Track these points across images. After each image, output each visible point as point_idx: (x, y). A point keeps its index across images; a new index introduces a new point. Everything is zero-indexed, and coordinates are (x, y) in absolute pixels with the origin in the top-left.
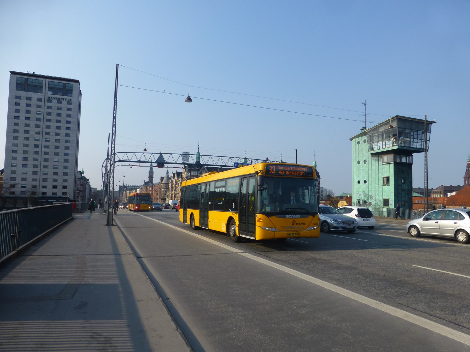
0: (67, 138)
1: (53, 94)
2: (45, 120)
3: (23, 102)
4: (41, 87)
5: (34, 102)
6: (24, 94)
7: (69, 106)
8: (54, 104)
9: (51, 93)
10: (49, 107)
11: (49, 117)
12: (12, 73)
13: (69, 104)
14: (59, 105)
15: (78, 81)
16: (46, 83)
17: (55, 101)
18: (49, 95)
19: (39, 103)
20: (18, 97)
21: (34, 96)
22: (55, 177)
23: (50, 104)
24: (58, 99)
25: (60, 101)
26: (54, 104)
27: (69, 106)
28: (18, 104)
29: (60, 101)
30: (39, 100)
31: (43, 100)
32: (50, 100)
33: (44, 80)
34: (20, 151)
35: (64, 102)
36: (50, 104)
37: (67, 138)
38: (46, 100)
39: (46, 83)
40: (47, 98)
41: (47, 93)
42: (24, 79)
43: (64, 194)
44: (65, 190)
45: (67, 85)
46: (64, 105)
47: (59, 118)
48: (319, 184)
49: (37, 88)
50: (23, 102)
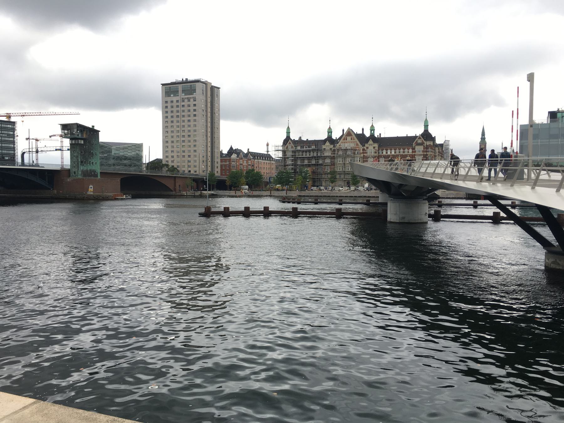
3: (169, 105)
5: (175, 104)
6: (169, 99)
7: (195, 103)
8: (186, 103)
9: (183, 94)
10: (183, 106)
12: (163, 85)
14: (189, 103)
17: (186, 100)
18: (183, 97)
20: (166, 102)
23: (183, 104)
24: (188, 98)
25: (189, 101)
26: (186, 103)
27: (195, 103)
28: (167, 107)
29: (189, 101)
30: (177, 101)
32: (183, 101)
35: (192, 100)
36: (183, 104)
49: (176, 93)
50: (169, 105)
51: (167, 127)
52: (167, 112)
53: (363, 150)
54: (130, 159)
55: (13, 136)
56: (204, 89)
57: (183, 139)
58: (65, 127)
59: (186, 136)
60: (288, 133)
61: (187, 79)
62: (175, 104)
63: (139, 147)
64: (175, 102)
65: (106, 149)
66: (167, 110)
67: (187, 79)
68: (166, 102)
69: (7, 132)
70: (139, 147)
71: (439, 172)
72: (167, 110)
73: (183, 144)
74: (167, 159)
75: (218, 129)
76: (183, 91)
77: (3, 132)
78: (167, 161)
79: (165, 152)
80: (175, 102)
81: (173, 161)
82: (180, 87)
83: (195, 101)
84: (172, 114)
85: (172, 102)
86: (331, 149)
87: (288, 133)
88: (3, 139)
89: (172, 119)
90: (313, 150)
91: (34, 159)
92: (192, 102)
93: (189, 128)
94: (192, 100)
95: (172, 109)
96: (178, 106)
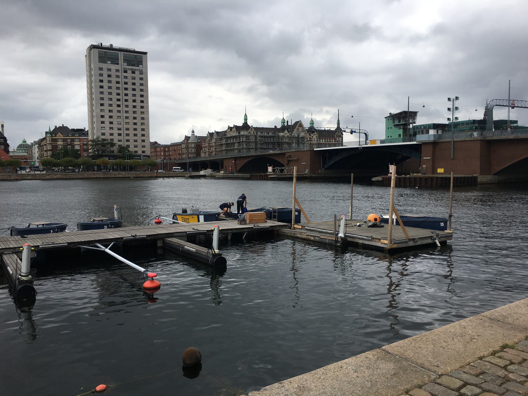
0: (142, 104)
1: (128, 65)
2: (123, 89)
4: (118, 59)
5: (113, 73)
6: (104, 66)
7: (141, 76)
8: (129, 74)
9: (126, 64)
10: (126, 77)
11: (126, 86)
13: (140, 74)
14: (133, 75)
15: (146, 53)
16: (121, 55)
17: (129, 72)
18: (125, 67)
19: (118, 74)
20: (101, 69)
21: (114, 67)
22: (136, 138)
25: (133, 72)
26: (129, 74)
27: (141, 76)
28: (101, 75)
29: (133, 72)
30: (117, 71)
31: (120, 71)
32: (125, 72)
33: (119, 52)
34: (107, 117)
36: (126, 74)
37: (142, 104)
38: (123, 71)
40: (123, 69)
41: (122, 65)
42: (103, 53)
43: (143, 152)
44: (144, 149)
45: (138, 57)
46: (137, 75)
47: (134, 87)
48: (342, 139)
49: (115, 61)
50: (105, 73)
53: (310, 138)
57: (127, 115)
60: (246, 119)
64: (113, 70)
67: (111, 45)
73: (127, 121)
76: (124, 60)
80: (113, 70)
85: (109, 70)
86: (288, 136)
87: (246, 119)
90: (271, 137)
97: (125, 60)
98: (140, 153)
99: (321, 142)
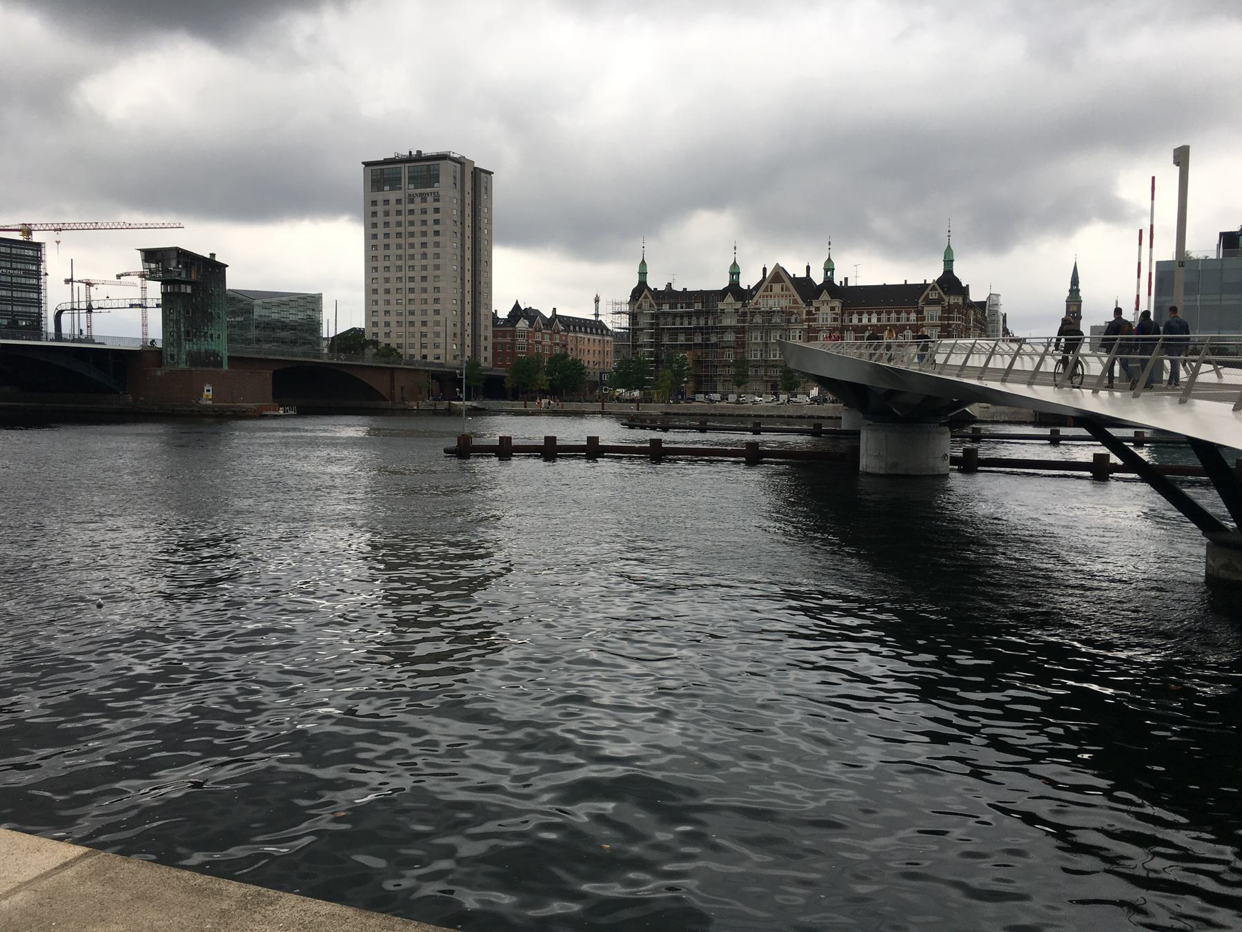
3: (380, 209)
5: (393, 207)
6: (380, 196)
7: (437, 205)
9: (412, 186)
10: (411, 212)
12: (367, 164)
14: (424, 205)
17: (417, 200)
18: (410, 192)
20: (374, 203)
21: (393, 196)
23: (411, 206)
24: (421, 194)
25: (424, 200)
26: (417, 205)
27: (437, 205)
28: (374, 214)
29: (424, 200)
30: (399, 201)
32: (412, 201)
35: (430, 199)
36: (411, 206)
39: (405, 169)
49: (394, 183)
50: (380, 209)
51: (375, 258)
52: (375, 225)
53: (809, 313)
54: (293, 328)
55: (37, 275)
56: (458, 176)
57: (411, 285)
58: (150, 255)
59: (418, 279)
60: (643, 274)
61: (419, 152)
62: (393, 207)
63: (314, 302)
64: (393, 202)
65: (241, 305)
66: (375, 220)
67: (419, 152)
68: (374, 203)
69: (23, 266)
70: (314, 302)
71: (999, 366)
72: (375, 220)
73: (412, 296)
74: (375, 330)
75: (489, 263)
76: (410, 178)
77: (14, 265)
78: (376, 334)
79: (370, 312)
80: (393, 202)
81: (387, 335)
82: (405, 169)
83: (438, 200)
84: (387, 230)
85: (387, 202)
86: (737, 311)
87: (643, 274)
88: (14, 280)
89: (386, 241)
90: (698, 314)
91: (84, 327)
92: (430, 204)
93: (424, 262)
94: (430, 199)
95: (387, 219)
96: (399, 213)
97: (412, 179)
98: (418, 358)
99: (865, 321)
